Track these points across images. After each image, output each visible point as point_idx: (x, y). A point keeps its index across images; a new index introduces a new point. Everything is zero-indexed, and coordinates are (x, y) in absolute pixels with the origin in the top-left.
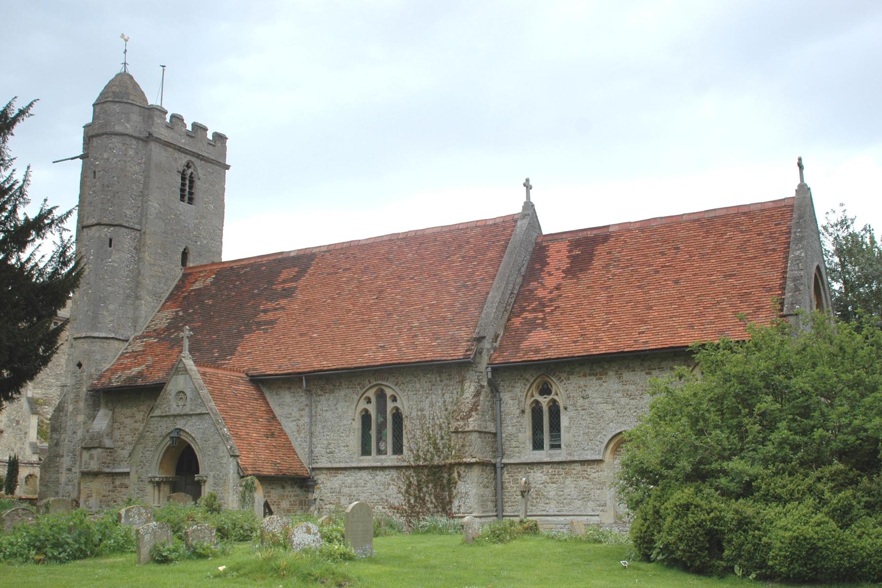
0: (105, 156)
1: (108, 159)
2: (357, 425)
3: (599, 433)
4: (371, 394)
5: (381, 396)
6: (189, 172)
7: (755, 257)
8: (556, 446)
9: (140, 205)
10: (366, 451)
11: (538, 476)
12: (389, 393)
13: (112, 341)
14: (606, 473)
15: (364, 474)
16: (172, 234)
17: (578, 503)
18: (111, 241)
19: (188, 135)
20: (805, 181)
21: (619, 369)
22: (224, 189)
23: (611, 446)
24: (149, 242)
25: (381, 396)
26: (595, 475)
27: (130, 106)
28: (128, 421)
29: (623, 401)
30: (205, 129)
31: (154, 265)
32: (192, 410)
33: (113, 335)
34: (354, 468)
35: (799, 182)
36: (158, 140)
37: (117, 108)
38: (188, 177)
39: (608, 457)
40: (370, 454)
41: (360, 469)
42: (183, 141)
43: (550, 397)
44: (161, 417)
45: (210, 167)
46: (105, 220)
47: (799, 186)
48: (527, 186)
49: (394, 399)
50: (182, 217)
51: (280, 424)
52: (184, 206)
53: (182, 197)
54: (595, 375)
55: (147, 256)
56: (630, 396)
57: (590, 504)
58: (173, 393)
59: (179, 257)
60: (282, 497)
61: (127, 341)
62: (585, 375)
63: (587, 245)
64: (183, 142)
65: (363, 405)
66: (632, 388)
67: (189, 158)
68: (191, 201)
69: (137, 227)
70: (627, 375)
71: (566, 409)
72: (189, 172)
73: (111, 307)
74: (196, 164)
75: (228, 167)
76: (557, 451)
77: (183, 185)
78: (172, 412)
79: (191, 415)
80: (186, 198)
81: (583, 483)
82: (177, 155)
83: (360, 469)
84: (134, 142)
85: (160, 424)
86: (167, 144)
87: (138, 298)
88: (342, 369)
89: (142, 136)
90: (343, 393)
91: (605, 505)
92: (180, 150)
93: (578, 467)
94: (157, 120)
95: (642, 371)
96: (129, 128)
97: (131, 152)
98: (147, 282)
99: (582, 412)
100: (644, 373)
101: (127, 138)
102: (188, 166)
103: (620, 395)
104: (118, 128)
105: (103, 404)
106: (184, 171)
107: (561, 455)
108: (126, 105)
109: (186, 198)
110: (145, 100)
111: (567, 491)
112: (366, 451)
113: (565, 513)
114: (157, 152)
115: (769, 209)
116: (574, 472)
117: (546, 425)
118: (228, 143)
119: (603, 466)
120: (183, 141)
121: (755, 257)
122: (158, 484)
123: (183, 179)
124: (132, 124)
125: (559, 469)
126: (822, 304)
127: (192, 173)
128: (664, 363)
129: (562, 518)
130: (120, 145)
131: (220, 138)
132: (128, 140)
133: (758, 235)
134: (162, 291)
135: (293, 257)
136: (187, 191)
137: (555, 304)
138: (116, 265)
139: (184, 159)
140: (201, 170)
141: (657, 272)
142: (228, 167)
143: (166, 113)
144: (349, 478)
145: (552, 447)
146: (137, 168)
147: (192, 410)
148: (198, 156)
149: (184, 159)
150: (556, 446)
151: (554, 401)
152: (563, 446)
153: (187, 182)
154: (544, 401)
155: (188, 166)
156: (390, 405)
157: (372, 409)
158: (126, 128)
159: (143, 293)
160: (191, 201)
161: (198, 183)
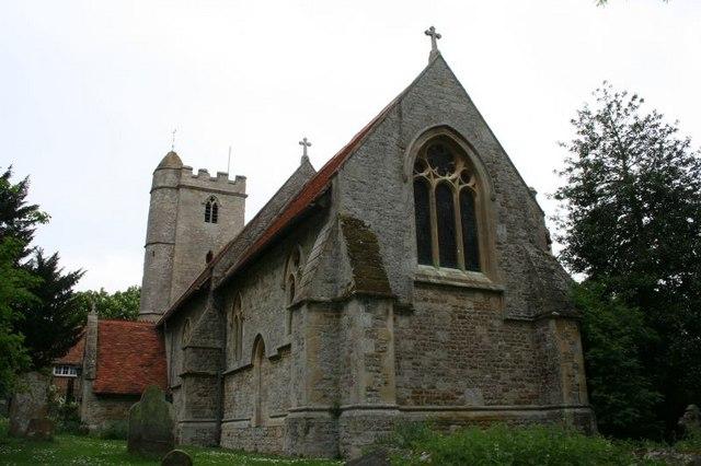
19: (212, 180)
52: (210, 225)
53: (207, 220)
55: (176, 259)
59: (204, 257)
67: (211, 194)
68: (215, 221)
73: (153, 294)
74: (219, 194)
86: (192, 188)
92: (203, 190)
98: (176, 275)
114: (184, 193)
118: (247, 181)
123: (208, 207)
124: (171, 179)
131: (241, 179)
140: (221, 201)
148: (219, 192)
149: (207, 196)
155: (212, 200)
160: (215, 221)
161: (220, 209)
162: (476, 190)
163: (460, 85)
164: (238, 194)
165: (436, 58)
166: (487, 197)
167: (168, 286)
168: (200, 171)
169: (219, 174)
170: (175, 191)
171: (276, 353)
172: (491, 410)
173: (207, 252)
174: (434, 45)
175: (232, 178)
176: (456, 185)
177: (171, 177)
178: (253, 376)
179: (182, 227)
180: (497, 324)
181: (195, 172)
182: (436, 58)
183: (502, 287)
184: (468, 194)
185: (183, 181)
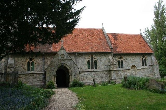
2: (87, 63)
4: (90, 57)
5: (92, 58)
8: (122, 67)
10: (89, 68)
11: (120, 72)
12: (94, 57)
15: (89, 73)
25: (92, 58)
28: (20, 61)
29: (133, 60)
34: (87, 72)
40: (97, 69)
41: (88, 72)
44: (56, 60)
49: (95, 58)
56: (133, 60)
58: (60, 55)
65: (88, 59)
70: (133, 57)
78: (60, 59)
79: (66, 60)
83: (88, 72)
85: (56, 62)
90: (83, 57)
105: (10, 56)
107: (124, 69)
112: (89, 68)
117: (121, 64)
122: (54, 76)
125: (123, 71)
144: (86, 74)
145: (122, 67)
150: (122, 67)
152: (124, 67)
154: (31, 62)
156: (94, 60)
157: (90, 60)
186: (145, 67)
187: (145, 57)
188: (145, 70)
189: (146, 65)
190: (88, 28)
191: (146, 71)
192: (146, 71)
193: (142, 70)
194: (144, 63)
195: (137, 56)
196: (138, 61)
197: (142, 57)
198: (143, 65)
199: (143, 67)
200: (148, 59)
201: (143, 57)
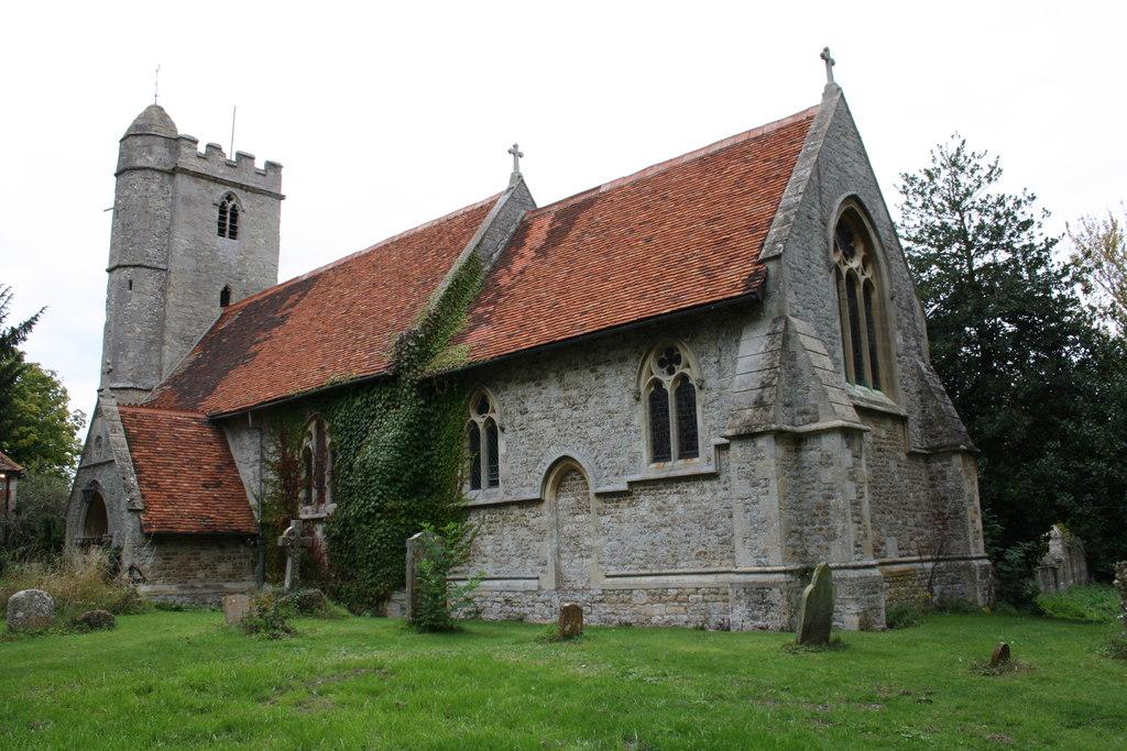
0: (127, 193)
1: (128, 197)
3: (539, 461)
6: (230, 205)
7: (752, 190)
8: (494, 483)
9: (166, 242)
13: (130, 391)
14: (545, 518)
16: (207, 272)
17: (516, 561)
18: (131, 282)
19: (229, 165)
20: (836, 80)
21: (561, 368)
22: (279, 221)
23: (551, 479)
24: (174, 282)
26: (533, 521)
27: (152, 138)
29: (566, 413)
30: (252, 158)
31: (182, 306)
32: (106, 457)
33: (131, 385)
35: (825, 81)
36: (185, 171)
37: (139, 141)
38: (228, 209)
39: (549, 496)
42: (221, 171)
43: (487, 415)
45: (259, 198)
46: (125, 262)
47: (827, 87)
48: (515, 153)
50: (220, 253)
51: (237, 471)
52: (226, 241)
53: (221, 232)
54: (534, 380)
55: (171, 298)
56: (574, 406)
57: (530, 562)
59: (217, 296)
60: (221, 559)
61: (150, 391)
62: (523, 382)
63: (573, 211)
64: (220, 172)
66: (574, 393)
67: (229, 189)
68: (233, 235)
69: (161, 266)
70: (570, 377)
71: (503, 430)
72: (232, 203)
73: (131, 355)
74: (241, 195)
75: (283, 197)
76: (495, 490)
77: (222, 218)
80: (227, 233)
81: (522, 532)
82: (212, 186)
84: (157, 175)
86: (197, 176)
87: (163, 343)
88: (281, 398)
89: (167, 168)
91: (545, 564)
92: (215, 180)
93: (517, 511)
94: (185, 150)
95: (586, 367)
96: (151, 161)
97: (154, 187)
98: (173, 325)
99: (520, 434)
100: (588, 371)
101: (148, 171)
102: (229, 198)
103: (560, 405)
104: (139, 163)
106: (223, 204)
107: (498, 495)
108: (148, 138)
109: (227, 233)
110: (174, 130)
111: (505, 544)
113: (504, 576)
114: (184, 184)
115: (787, 127)
116: (512, 517)
118: (283, 172)
119: (544, 507)
120: (221, 171)
121: (752, 190)
123: (223, 211)
124: (157, 156)
125: (497, 515)
126: (875, 255)
127: (234, 206)
128: (612, 353)
129: (498, 582)
130: (140, 180)
131: (273, 167)
132: (150, 174)
133: (765, 161)
134: (193, 334)
135: (305, 281)
136: (229, 223)
137: (511, 292)
138: (136, 309)
139: (222, 191)
140: (244, 202)
141: (632, 231)
142: (283, 197)
143: (196, 142)
146: (162, 203)
147: (106, 457)
148: (241, 187)
149: (222, 191)
151: (491, 420)
153: (228, 215)
155: (229, 198)
158: (148, 161)
159: (168, 337)
160: (233, 235)
161: (242, 217)
162: (874, 282)
163: (859, 138)
164: (270, 194)
165: (833, 91)
166: (887, 295)
167: (156, 341)
168: (208, 146)
169: (240, 156)
170: (166, 177)
171: (624, 487)
172: (907, 562)
173: (221, 289)
174: (830, 76)
175: (260, 164)
176: (859, 274)
177: (154, 155)
178: (543, 517)
179: (182, 241)
180: (903, 457)
181: (201, 148)
182: (833, 91)
183: (903, 412)
184: (868, 286)
185: (184, 162)
186: (677, 467)
187: (687, 354)
188: (672, 497)
189: (689, 448)
190: (446, 214)
191: (680, 509)
192: (680, 509)
193: (646, 504)
194: (673, 425)
195: (601, 369)
196: (604, 419)
197: (651, 362)
198: (660, 452)
199: (653, 471)
200: (734, 376)
201: (661, 364)
